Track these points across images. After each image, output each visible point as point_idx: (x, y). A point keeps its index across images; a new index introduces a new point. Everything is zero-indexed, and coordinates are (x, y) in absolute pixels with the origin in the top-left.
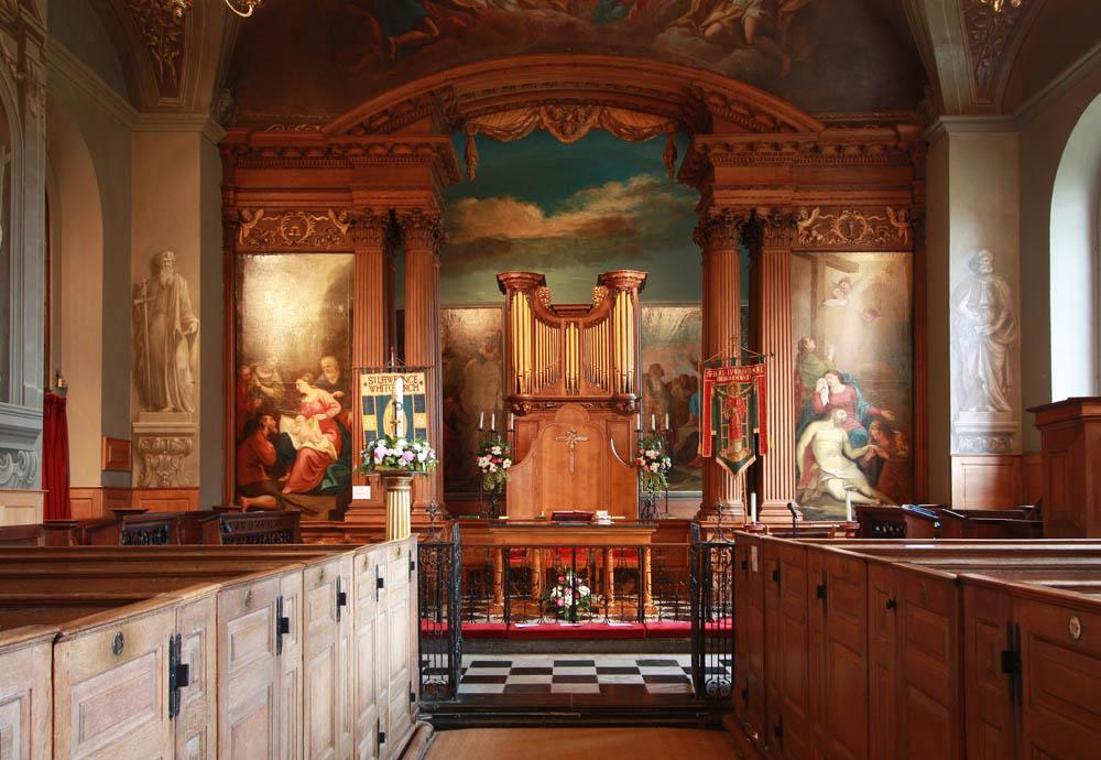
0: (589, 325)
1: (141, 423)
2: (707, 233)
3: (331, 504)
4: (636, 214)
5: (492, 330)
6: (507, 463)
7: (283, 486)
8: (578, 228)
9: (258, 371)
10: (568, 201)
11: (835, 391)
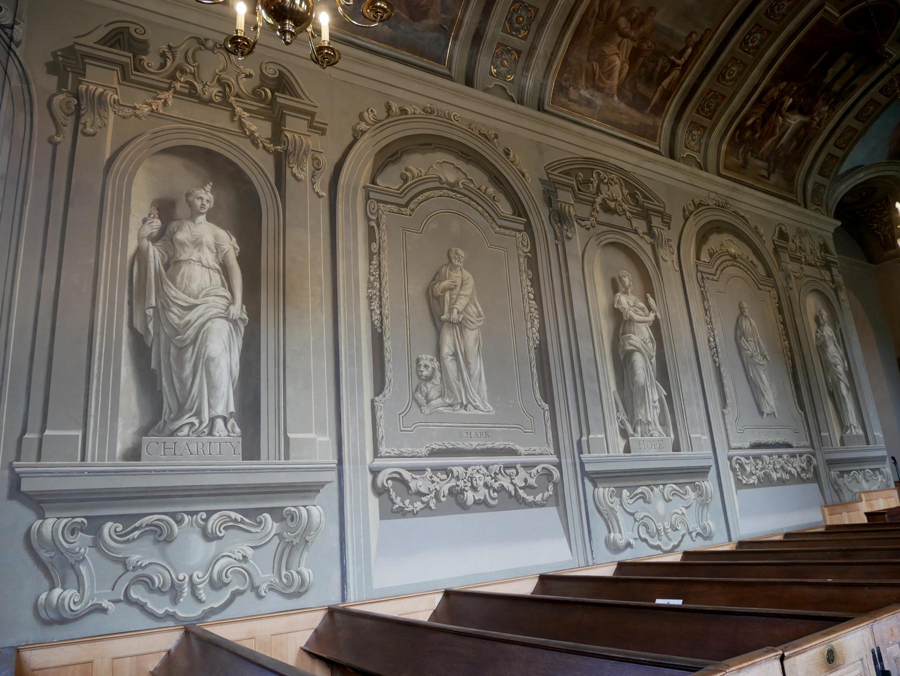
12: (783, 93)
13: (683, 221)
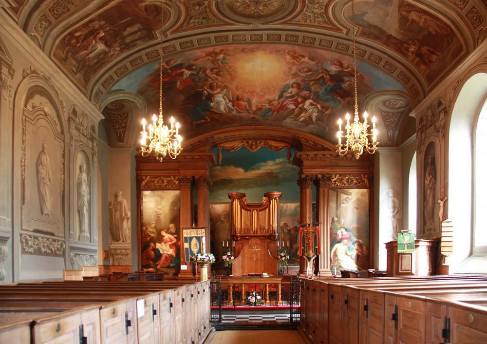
0: (260, 211)
1: (112, 245)
2: (302, 183)
3: (174, 271)
4: (278, 171)
5: (226, 212)
6: (232, 258)
7: (157, 265)
9: (148, 228)
10: (254, 167)
11: (344, 234)
12: (101, 27)
13: (22, 78)
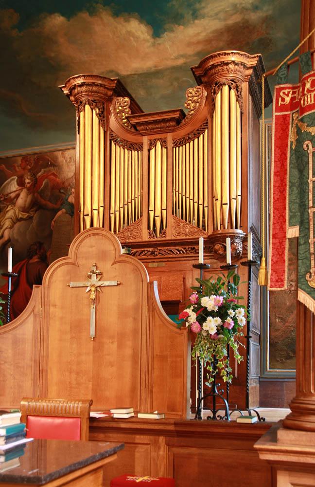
0: (179, 143)
8: (199, 48)
